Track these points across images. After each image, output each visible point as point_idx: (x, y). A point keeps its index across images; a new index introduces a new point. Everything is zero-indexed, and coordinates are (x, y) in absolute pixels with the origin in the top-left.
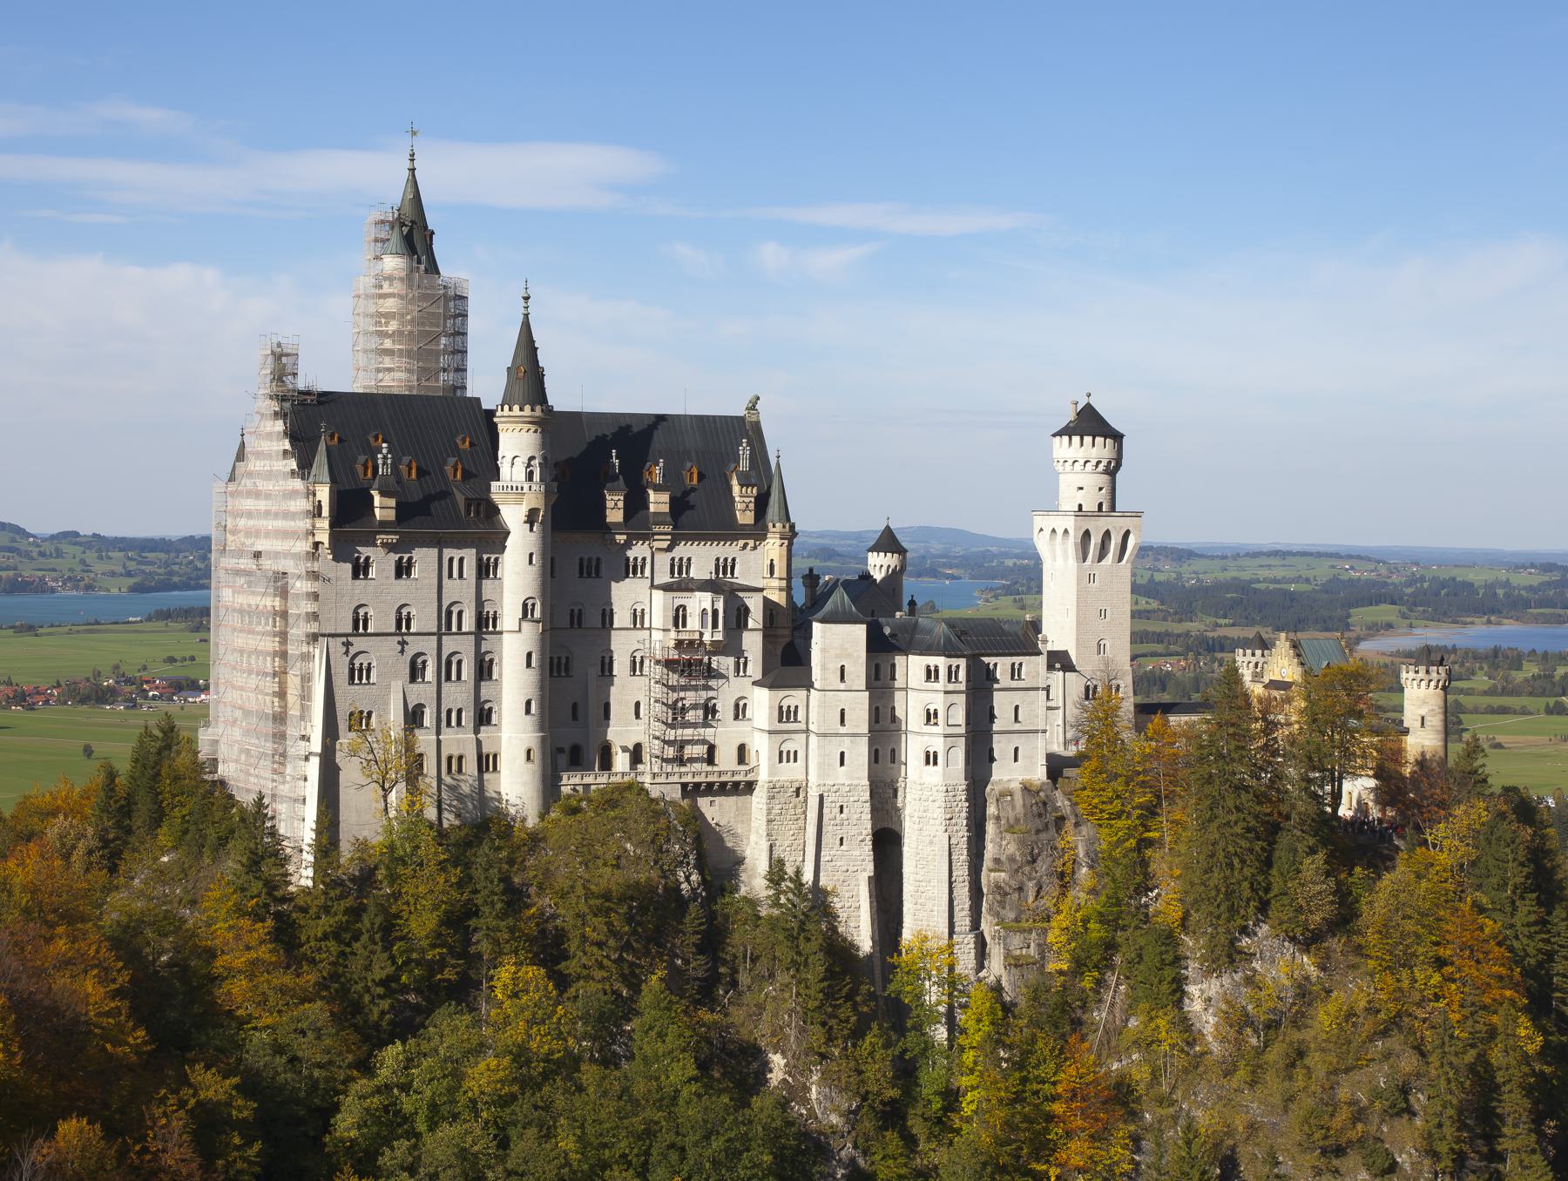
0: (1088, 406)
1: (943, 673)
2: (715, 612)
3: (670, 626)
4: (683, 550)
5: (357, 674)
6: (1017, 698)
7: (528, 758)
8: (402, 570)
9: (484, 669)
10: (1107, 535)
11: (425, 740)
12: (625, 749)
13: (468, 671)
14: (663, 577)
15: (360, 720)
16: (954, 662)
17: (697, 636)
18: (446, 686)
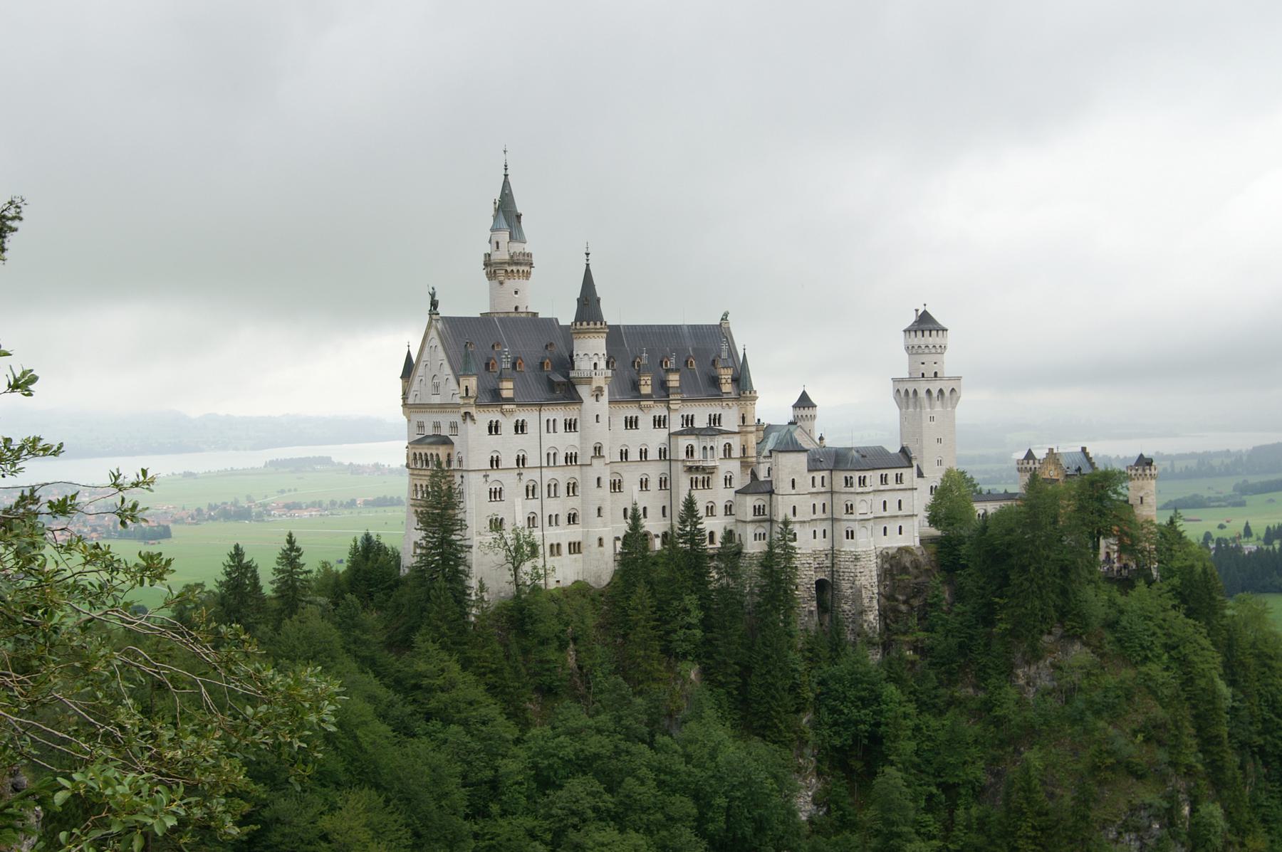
0: (925, 312)
1: (856, 480)
2: (712, 448)
3: (684, 457)
4: (689, 410)
5: (496, 494)
6: (900, 495)
7: (601, 545)
8: (520, 428)
9: (572, 488)
10: (941, 391)
11: (537, 534)
12: (657, 536)
13: (562, 489)
14: (676, 424)
15: (497, 525)
16: (862, 474)
17: (701, 464)
18: (547, 501)
